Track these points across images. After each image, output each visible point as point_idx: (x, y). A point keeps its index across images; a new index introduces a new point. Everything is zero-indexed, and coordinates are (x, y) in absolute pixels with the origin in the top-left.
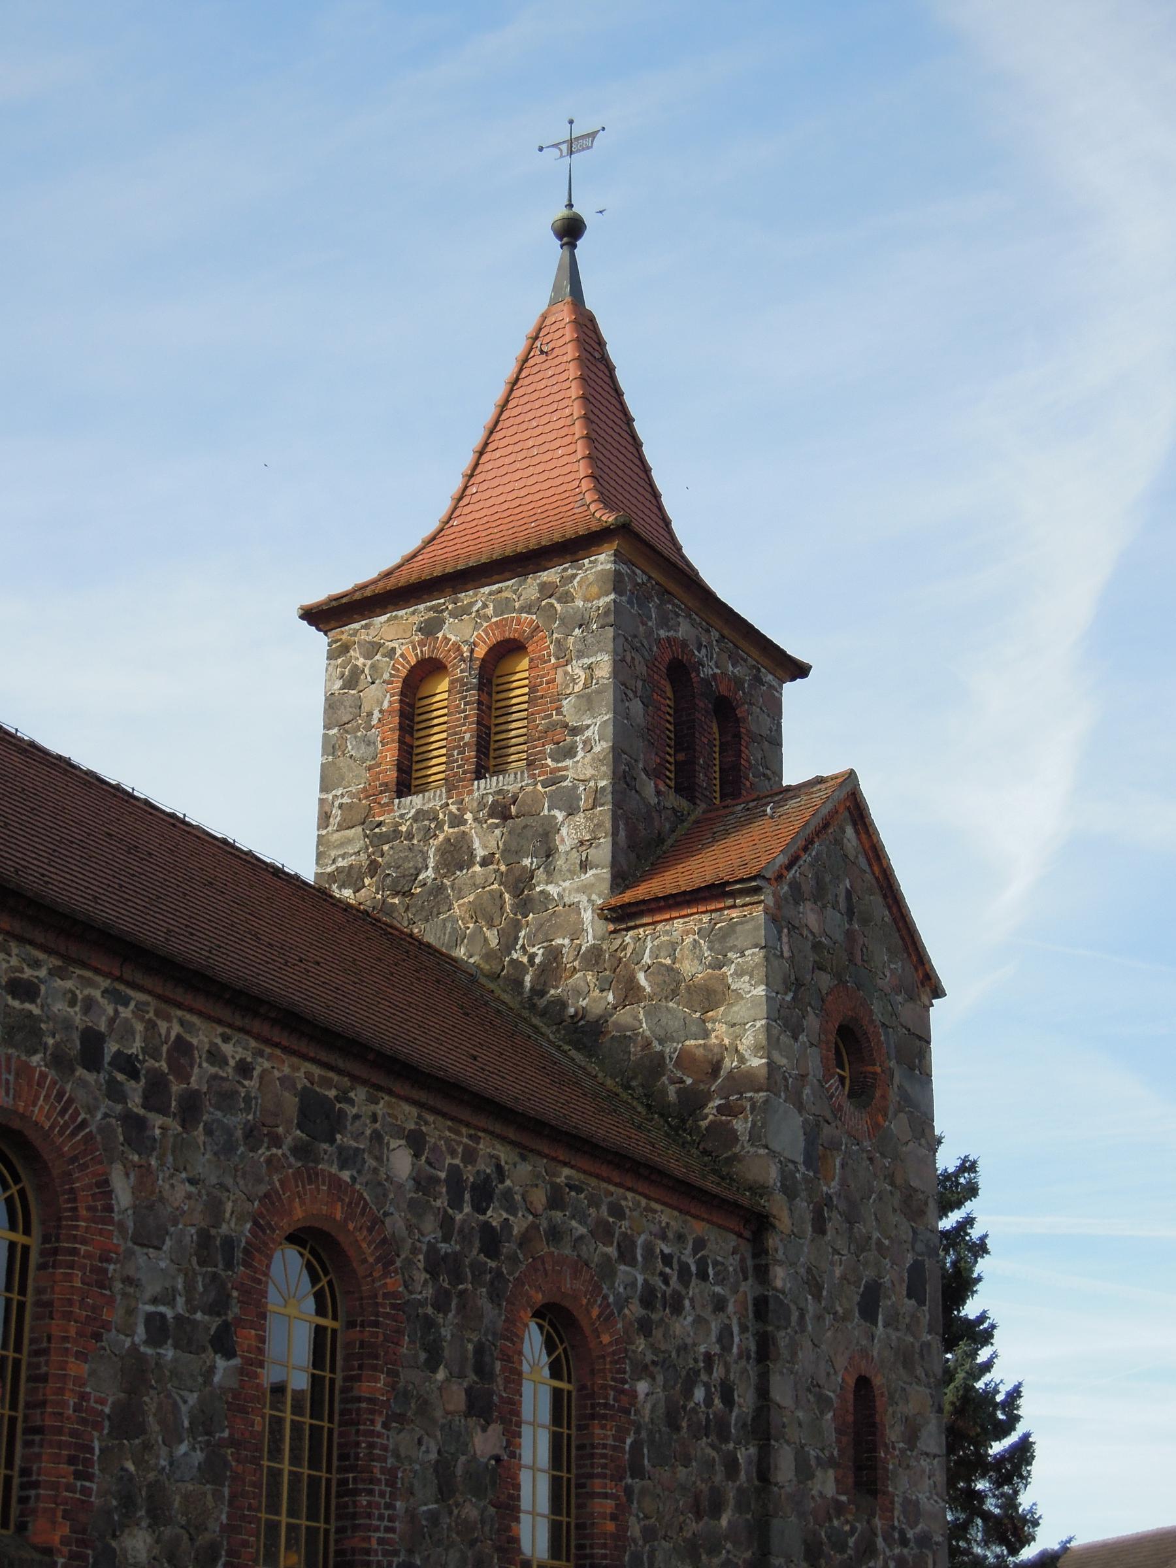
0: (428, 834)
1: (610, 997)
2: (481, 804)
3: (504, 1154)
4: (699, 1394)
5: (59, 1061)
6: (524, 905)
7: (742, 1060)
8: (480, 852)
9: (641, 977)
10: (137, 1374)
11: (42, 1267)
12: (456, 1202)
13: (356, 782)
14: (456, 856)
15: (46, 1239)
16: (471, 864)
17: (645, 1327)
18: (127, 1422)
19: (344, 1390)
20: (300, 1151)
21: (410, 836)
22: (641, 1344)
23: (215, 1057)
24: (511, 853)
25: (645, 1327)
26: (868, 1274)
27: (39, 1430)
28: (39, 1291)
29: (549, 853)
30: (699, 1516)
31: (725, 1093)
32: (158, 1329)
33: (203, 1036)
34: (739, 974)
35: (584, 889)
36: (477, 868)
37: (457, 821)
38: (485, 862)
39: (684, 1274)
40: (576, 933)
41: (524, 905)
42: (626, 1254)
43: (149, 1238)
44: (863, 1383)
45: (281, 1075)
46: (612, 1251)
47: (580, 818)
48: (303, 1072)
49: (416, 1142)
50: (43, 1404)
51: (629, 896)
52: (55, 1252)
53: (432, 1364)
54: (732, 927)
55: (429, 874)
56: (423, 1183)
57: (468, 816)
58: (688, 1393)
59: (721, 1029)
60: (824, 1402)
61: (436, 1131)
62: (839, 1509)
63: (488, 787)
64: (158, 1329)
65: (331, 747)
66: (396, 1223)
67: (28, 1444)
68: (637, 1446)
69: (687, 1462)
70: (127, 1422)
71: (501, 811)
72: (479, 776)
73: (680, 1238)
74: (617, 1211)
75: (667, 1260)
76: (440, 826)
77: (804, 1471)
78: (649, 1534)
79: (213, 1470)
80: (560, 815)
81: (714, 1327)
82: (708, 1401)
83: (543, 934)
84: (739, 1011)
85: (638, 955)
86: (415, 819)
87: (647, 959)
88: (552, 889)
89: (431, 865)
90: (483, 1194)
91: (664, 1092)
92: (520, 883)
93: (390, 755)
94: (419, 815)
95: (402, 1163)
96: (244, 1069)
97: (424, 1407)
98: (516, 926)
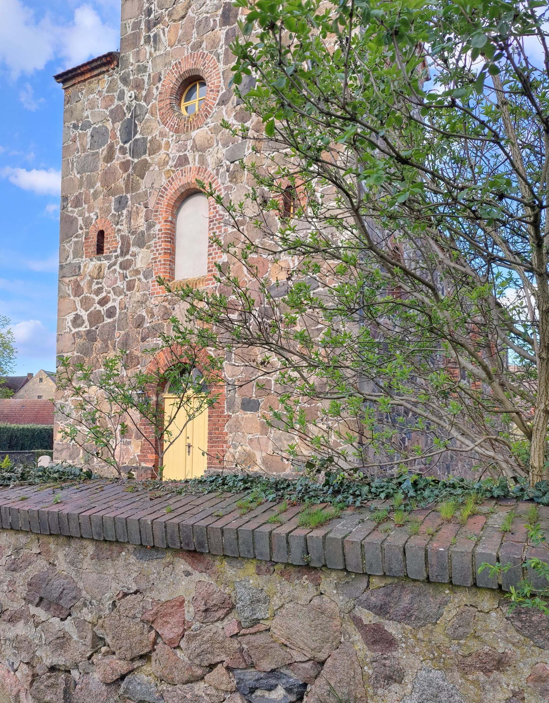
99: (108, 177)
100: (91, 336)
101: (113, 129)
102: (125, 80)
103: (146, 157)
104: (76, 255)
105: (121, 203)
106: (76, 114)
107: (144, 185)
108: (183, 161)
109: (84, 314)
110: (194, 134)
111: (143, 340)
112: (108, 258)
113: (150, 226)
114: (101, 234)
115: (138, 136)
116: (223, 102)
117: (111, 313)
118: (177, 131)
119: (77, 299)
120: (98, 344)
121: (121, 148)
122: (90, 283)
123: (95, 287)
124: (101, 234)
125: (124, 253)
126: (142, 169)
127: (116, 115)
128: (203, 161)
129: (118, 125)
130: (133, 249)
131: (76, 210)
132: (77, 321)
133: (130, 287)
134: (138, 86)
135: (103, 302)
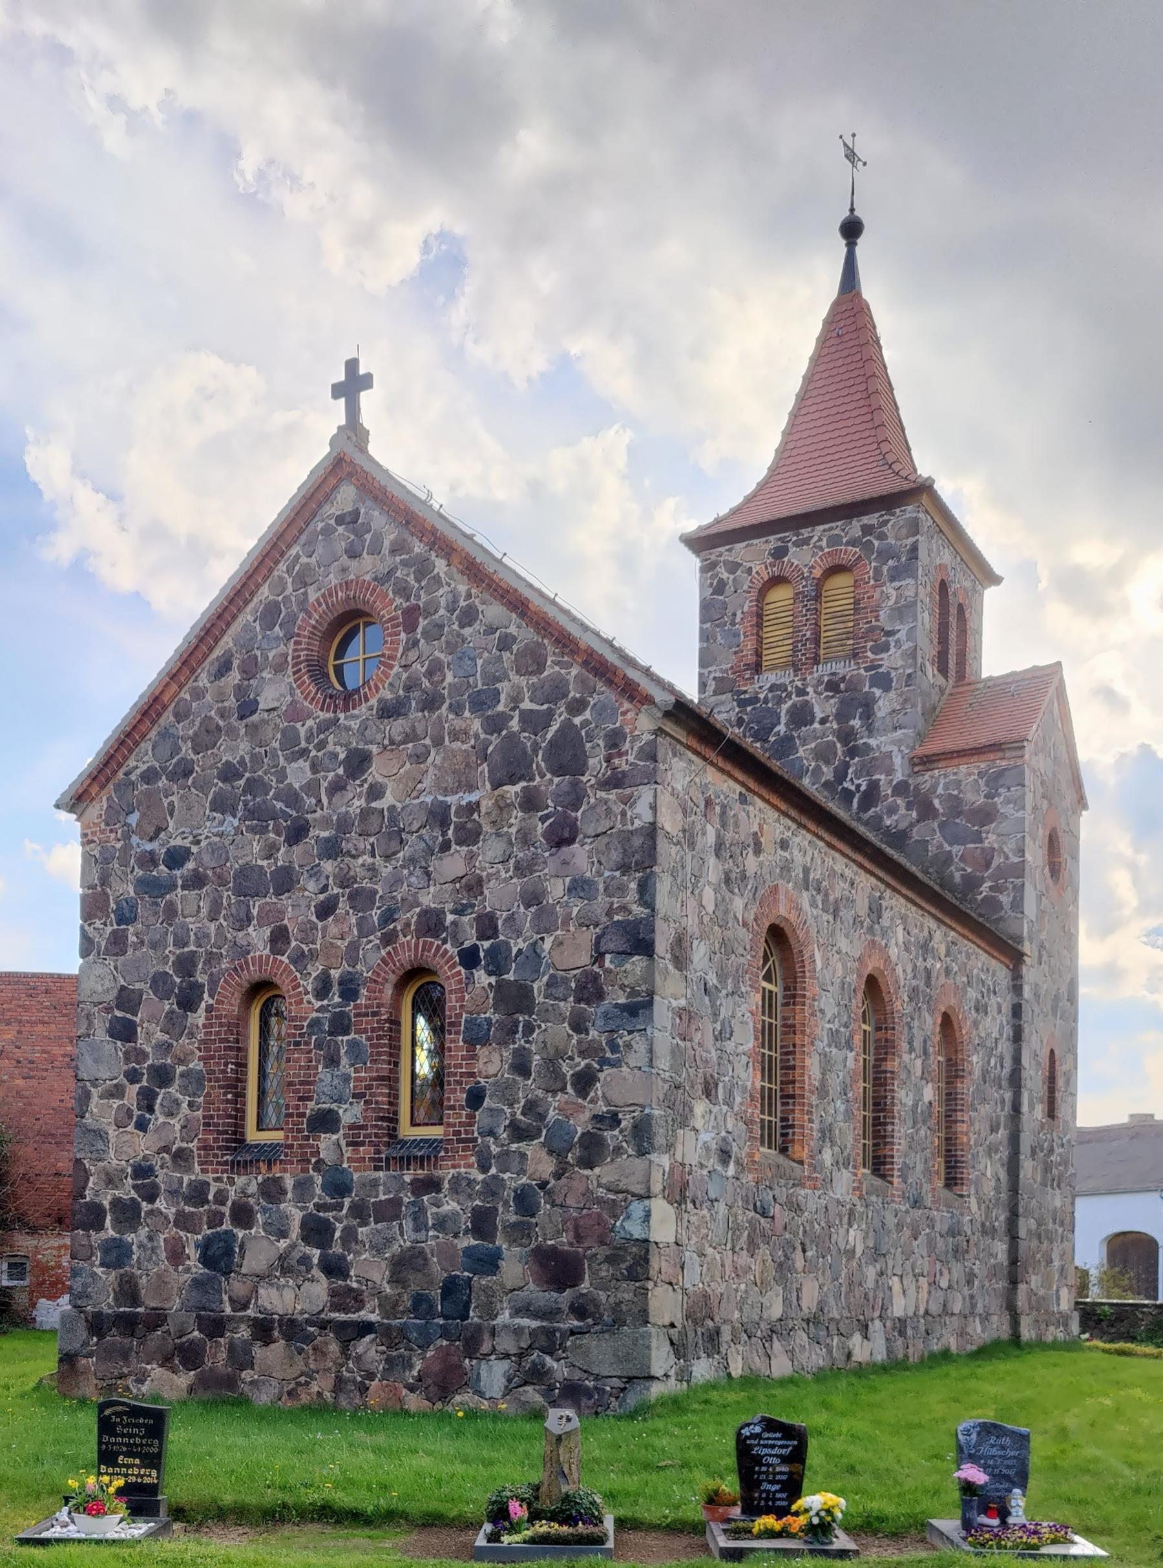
0: (780, 701)
1: (914, 814)
2: (820, 682)
6: (852, 752)
7: (1007, 858)
8: (819, 715)
9: (936, 802)
11: (784, 1005)
13: (726, 663)
14: (801, 716)
15: (786, 988)
16: (812, 723)
19: (875, 1066)
21: (766, 701)
24: (842, 716)
27: (793, 1097)
28: (784, 1018)
29: (868, 714)
31: (995, 877)
34: (1008, 801)
35: (898, 742)
36: (816, 725)
37: (801, 692)
38: (823, 721)
40: (890, 771)
41: (852, 752)
44: (1052, 1051)
47: (892, 694)
50: (794, 1082)
51: (931, 748)
52: (794, 996)
54: (1001, 773)
55: (781, 728)
57: (810, 689)
59: (992, 837)
63: (823, 671)
65: (705, 637)
67: (783, 1104)
71: (833, 686)
72: (816, 660)
76: (789, 696)
80: (877, 692)
81: (998, 1021)
83: (866, 770)
84: (1004, 827)
85: (934, 787)
86: (771, 689)
87: (940, 790)
88: (873, 742)
89: (783, 720)
91: (952, 876)
92: (847, 736)
93: (749, 646)
94: (772, 688)
98: (847, 765)
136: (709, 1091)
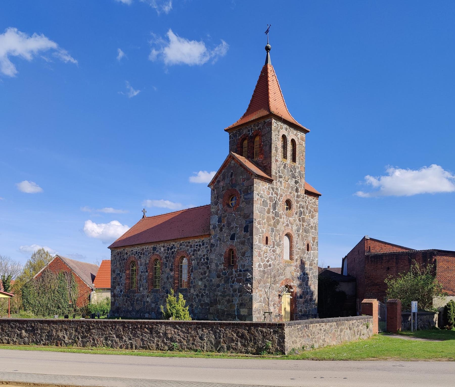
3: (174, 243)
4: (202, 260)
5: (135, 255)
10: (141, 276)
12: (168, 250)
17: (193, 255)
18: (140, 280)
20: (153, 253)
22: (193, 257)
23: (146, 248)
25: (193, 255)
26: (232, 233)
30: (202, 275)
32: (142, 272)
33: (144, 247)
39: (200, 246)
42: (191, 247)
43: (141, 265)
45: (150, 247)
46: (189, 248)
48: (153, 246)
49: (164, 247)
53: (166, 268)
56: (165, 250)
58: (201, 260)
60: (221, 255)
61: (166, 245)
62: (224, 269)
64: (142, 272)
66: (161, 255)
68: (192, 269)
69: (200, 269)
70: (140, 280)
73: (199, 242)
74: (189, 243)
75: (197, 245)
77: (217, 265)
78: (194, 278)
79: (146, 282)
82: (204, 260)
90: (172, 248)
95: (162, 249)
96: (148, 248)
97: (165, 272)
99: (268, 219)
100: (264, 272)
101: (270, 204)
102: (273, 189)
103: (278, 218)
104: (259, 242)
105: (272, 231)
106: (258, 190)
107: (278, 227)
108: (287, 225)
109: (262, 264)
110: (290, 218)
111: (279, 276)
112: (269, 247)
113: (280, 241)
114: (267, 238)
115: (277, 210)
116: (296, 214)
117: (270, 266)
118: (286, 215)
119: (260, 258)
120: (266, 275)
121: (272, 212)
122: (264, 254)
123: (265, 255)
124: (267, 238)
125: (273, 247)
126: (278, 222)
127: (271, 199)
128: (292, 228)
129: (272, 203)
130: (275, 247)
131: (259, 226)
132: (259, 265)
133: (275, 259)
134: (277, 194)
135: (268, 261)
136: (119, 285)
